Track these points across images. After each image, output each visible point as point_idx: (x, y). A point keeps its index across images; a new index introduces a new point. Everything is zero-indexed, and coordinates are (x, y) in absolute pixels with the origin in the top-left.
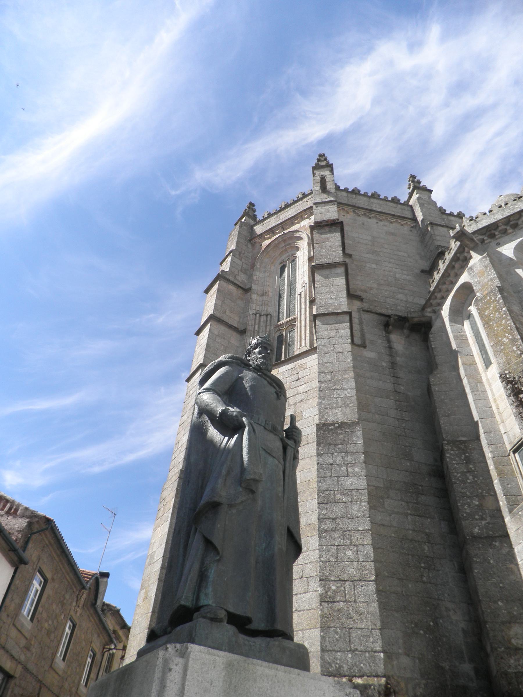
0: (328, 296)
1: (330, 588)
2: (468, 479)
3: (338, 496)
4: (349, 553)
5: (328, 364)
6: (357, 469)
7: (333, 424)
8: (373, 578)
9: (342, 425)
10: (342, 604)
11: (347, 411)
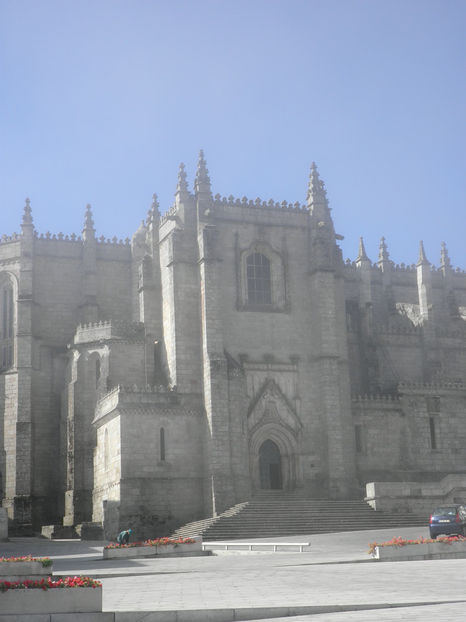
0: (23, 355)
1: (18, 475)
2: (65, 437)
3: (22, 449)
4: (24, 466)
5: (22, 395)
6: (28, 440)
7: (22, 423)
8: (30, 472)
9: (25, 423)
10: (21, 479)
11: (27, 417)
